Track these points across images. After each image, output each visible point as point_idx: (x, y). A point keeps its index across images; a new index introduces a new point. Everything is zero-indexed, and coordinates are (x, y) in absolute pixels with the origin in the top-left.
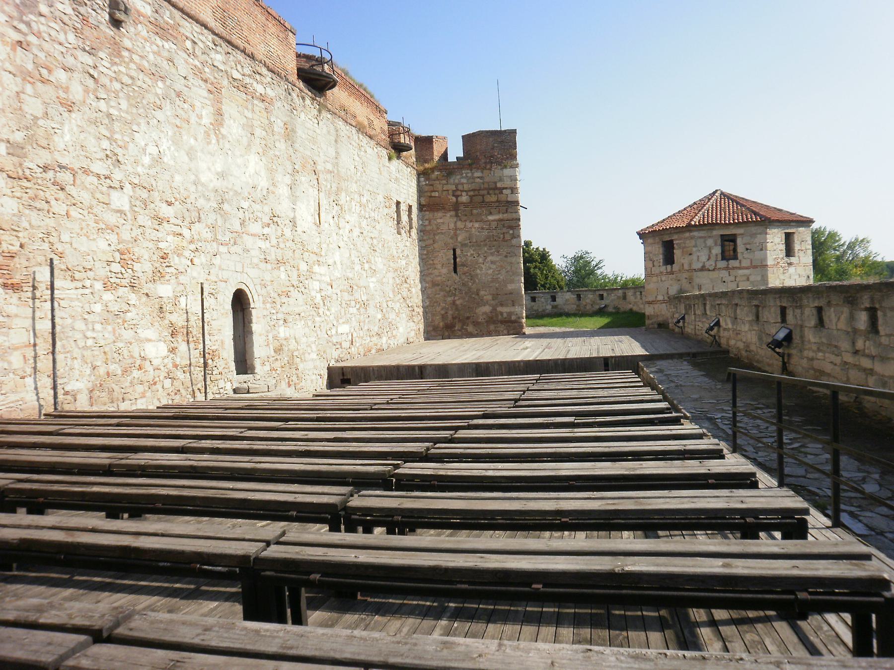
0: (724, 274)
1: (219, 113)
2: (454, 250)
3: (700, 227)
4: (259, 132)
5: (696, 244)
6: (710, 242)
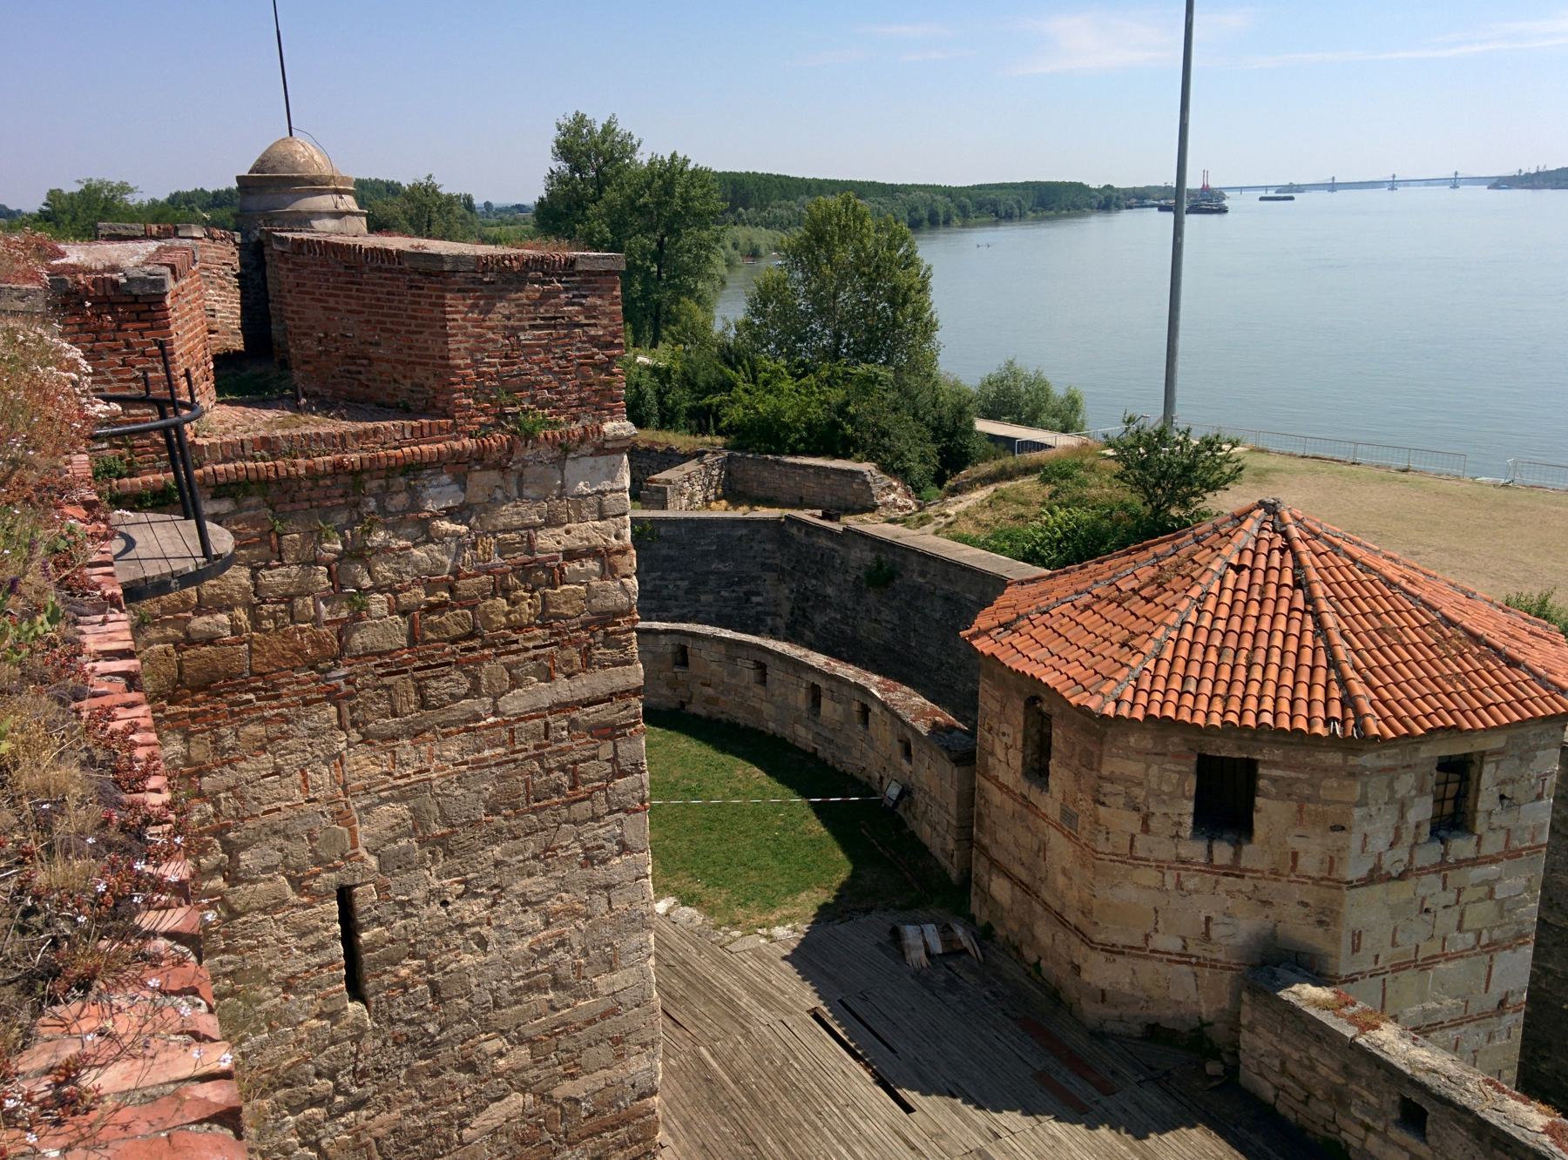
2: (345, 896)
5: (1364, 795)
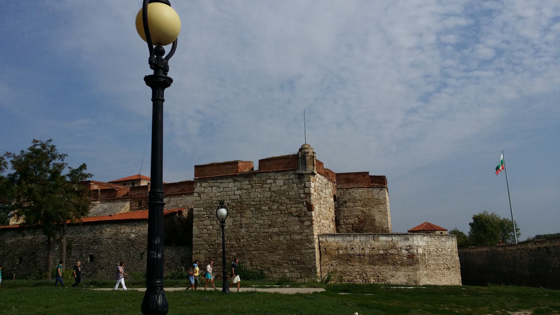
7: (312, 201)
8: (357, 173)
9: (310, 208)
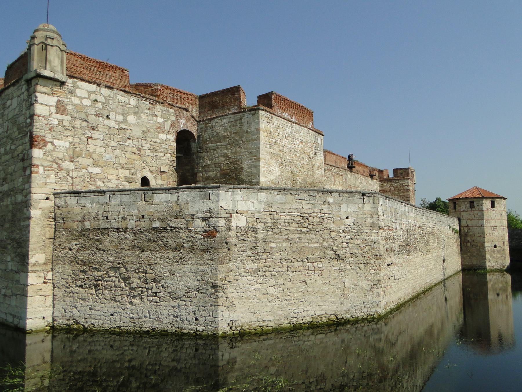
0: (470, 213)
1: (335, 180)
3: (463, 198)
4: (341, 182)
6: (466, 203)
7: (34, 130)
8: (224, 90)
9: (32, 142)
